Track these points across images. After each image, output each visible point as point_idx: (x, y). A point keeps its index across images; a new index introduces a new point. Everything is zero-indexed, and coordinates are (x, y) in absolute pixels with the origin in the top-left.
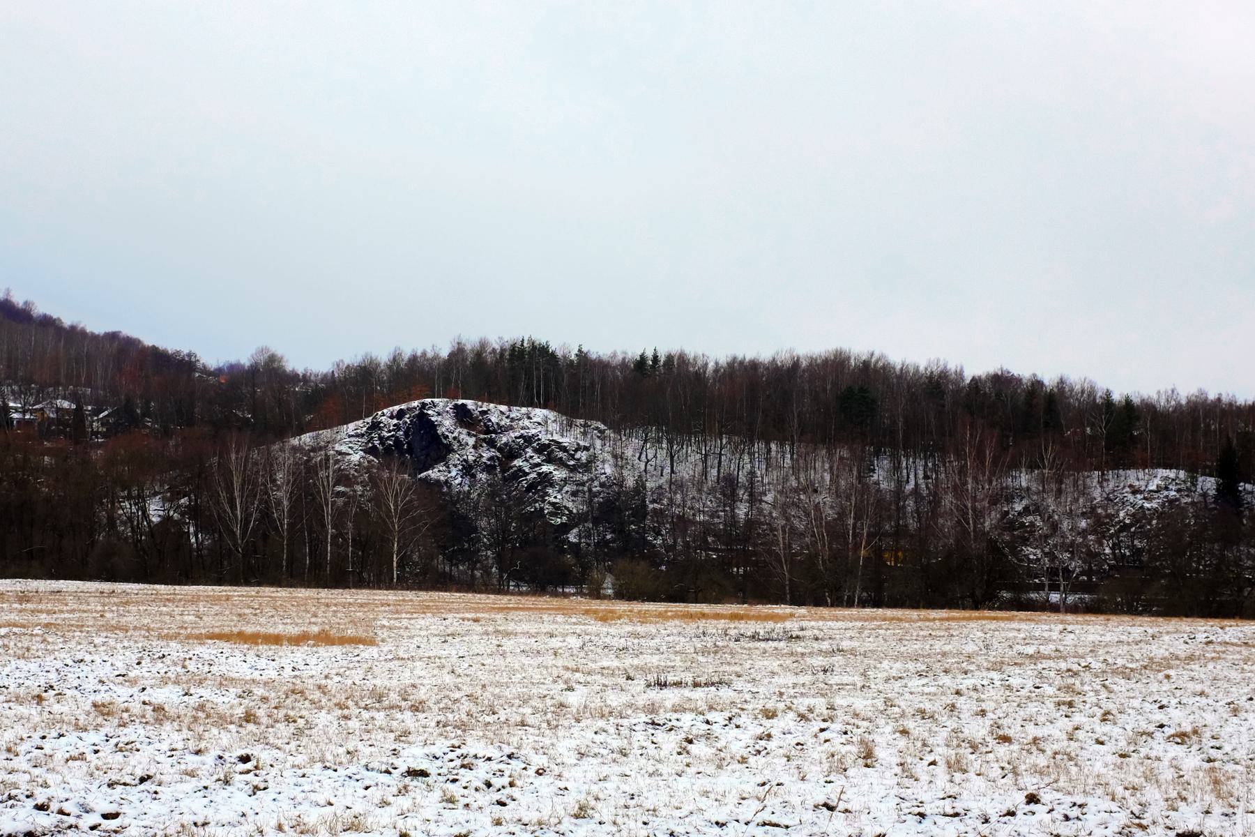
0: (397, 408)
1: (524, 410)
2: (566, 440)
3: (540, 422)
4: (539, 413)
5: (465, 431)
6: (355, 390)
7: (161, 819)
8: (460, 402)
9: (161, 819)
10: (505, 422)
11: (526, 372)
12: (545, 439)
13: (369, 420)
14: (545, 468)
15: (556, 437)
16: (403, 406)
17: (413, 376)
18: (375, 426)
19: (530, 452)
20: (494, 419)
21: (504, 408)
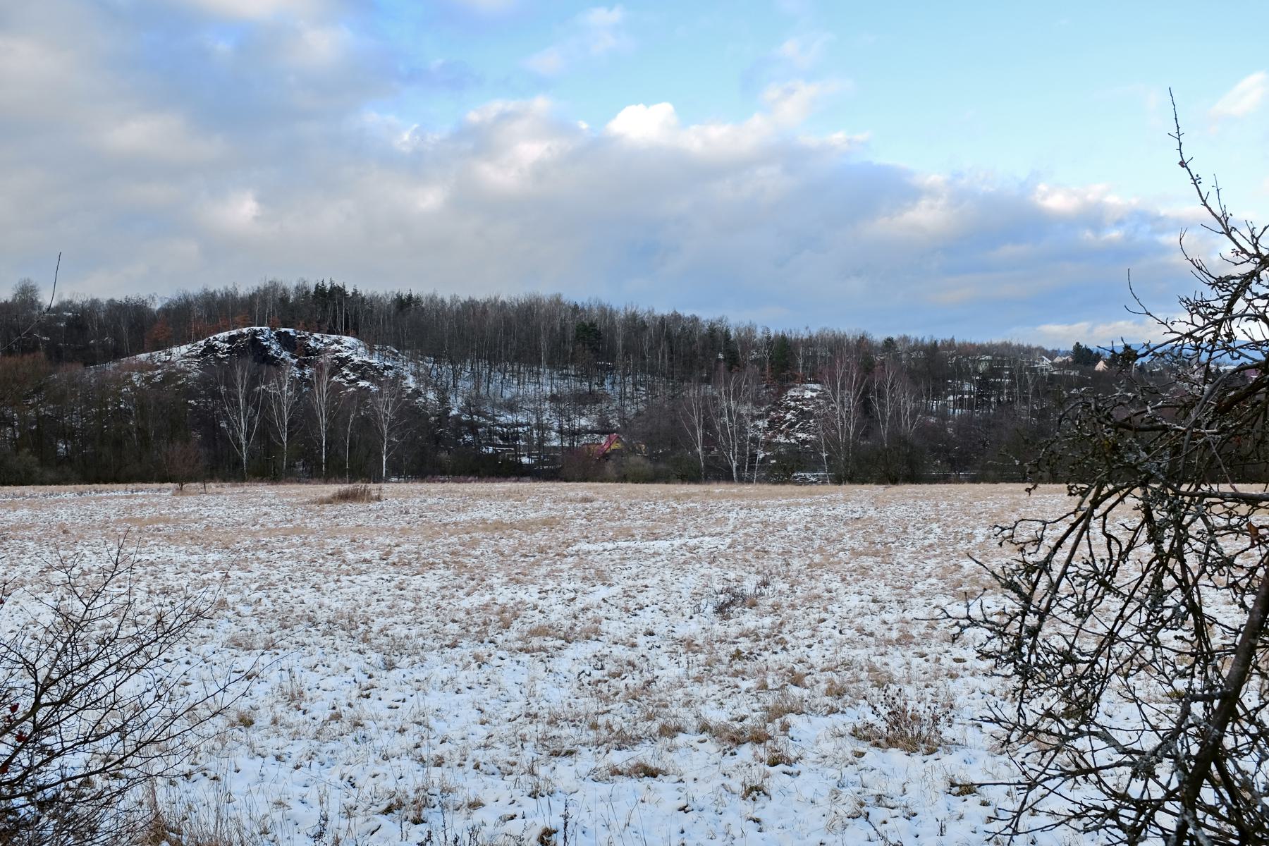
0: (226, 334)
1: (334, 337)
2: (375, 361)
3: (349, 346)
4: (349, 340)
5: (288, 353)
6: (182, 320)
7: (543, 704)
8: (283, 330)
9: (543, 704)
10: (320, 346)
11: (331, 307)
12: (357, 359)
13: (202, 342)
14: (362, 384)
15: (366, 359)
16: (234, 332)
17: (219, 310)
18: (210, 349)
19: (346, 371)
20: (312, 344)
21: (317, 335)
